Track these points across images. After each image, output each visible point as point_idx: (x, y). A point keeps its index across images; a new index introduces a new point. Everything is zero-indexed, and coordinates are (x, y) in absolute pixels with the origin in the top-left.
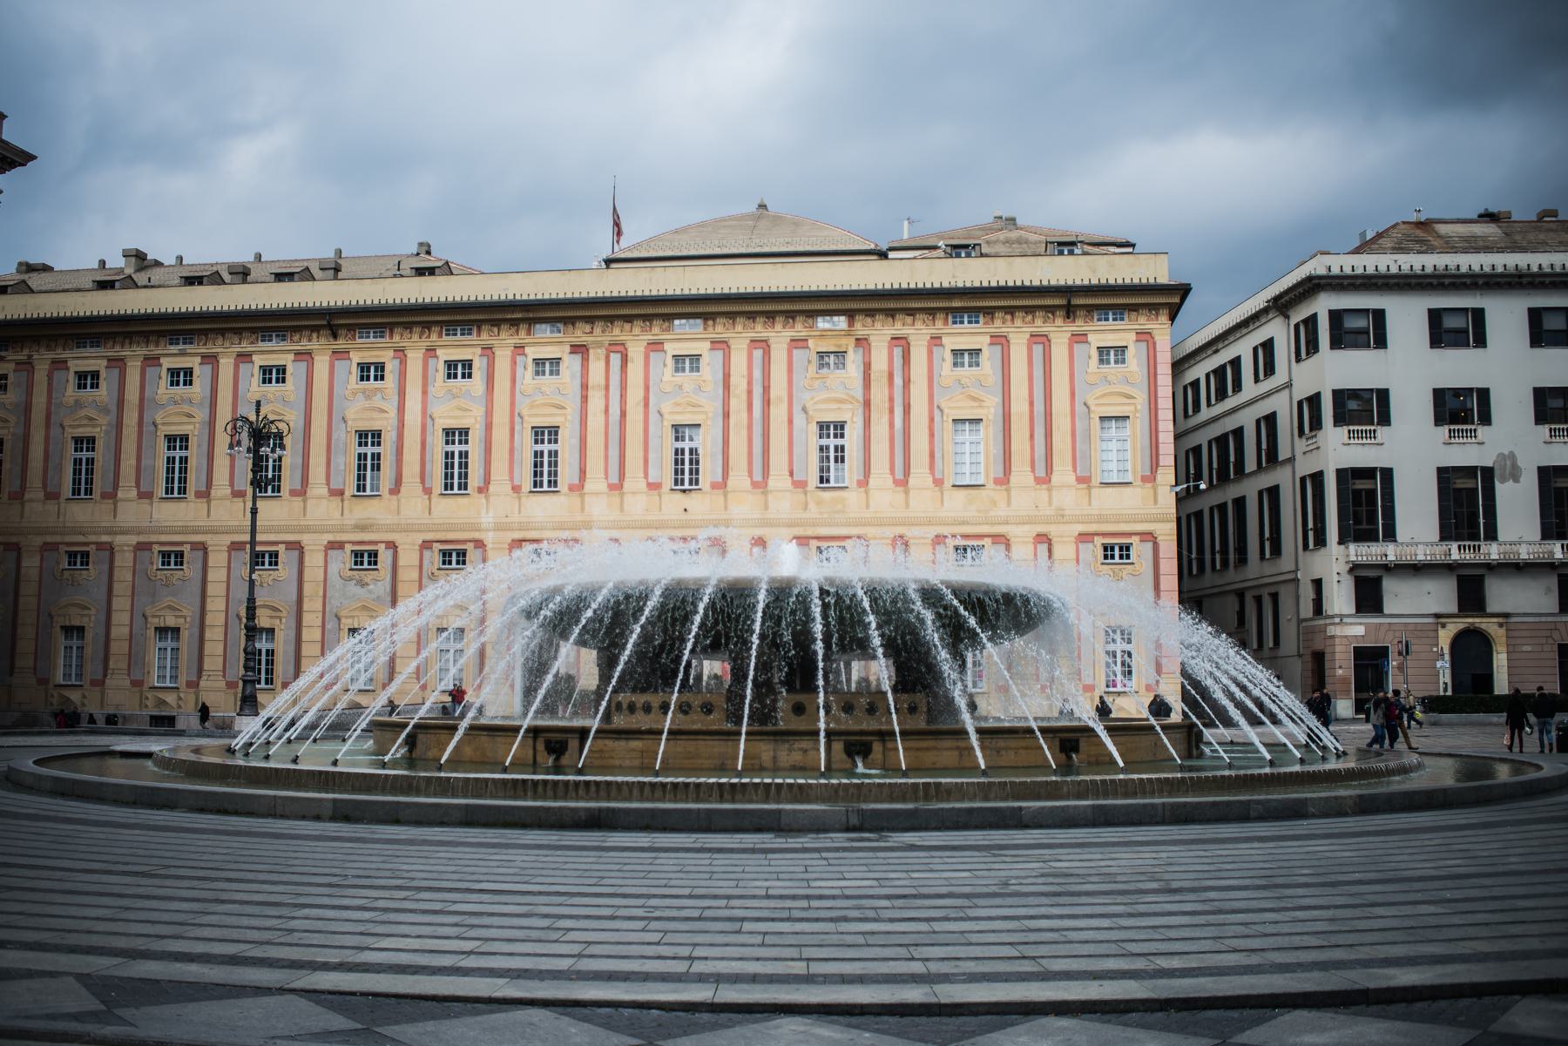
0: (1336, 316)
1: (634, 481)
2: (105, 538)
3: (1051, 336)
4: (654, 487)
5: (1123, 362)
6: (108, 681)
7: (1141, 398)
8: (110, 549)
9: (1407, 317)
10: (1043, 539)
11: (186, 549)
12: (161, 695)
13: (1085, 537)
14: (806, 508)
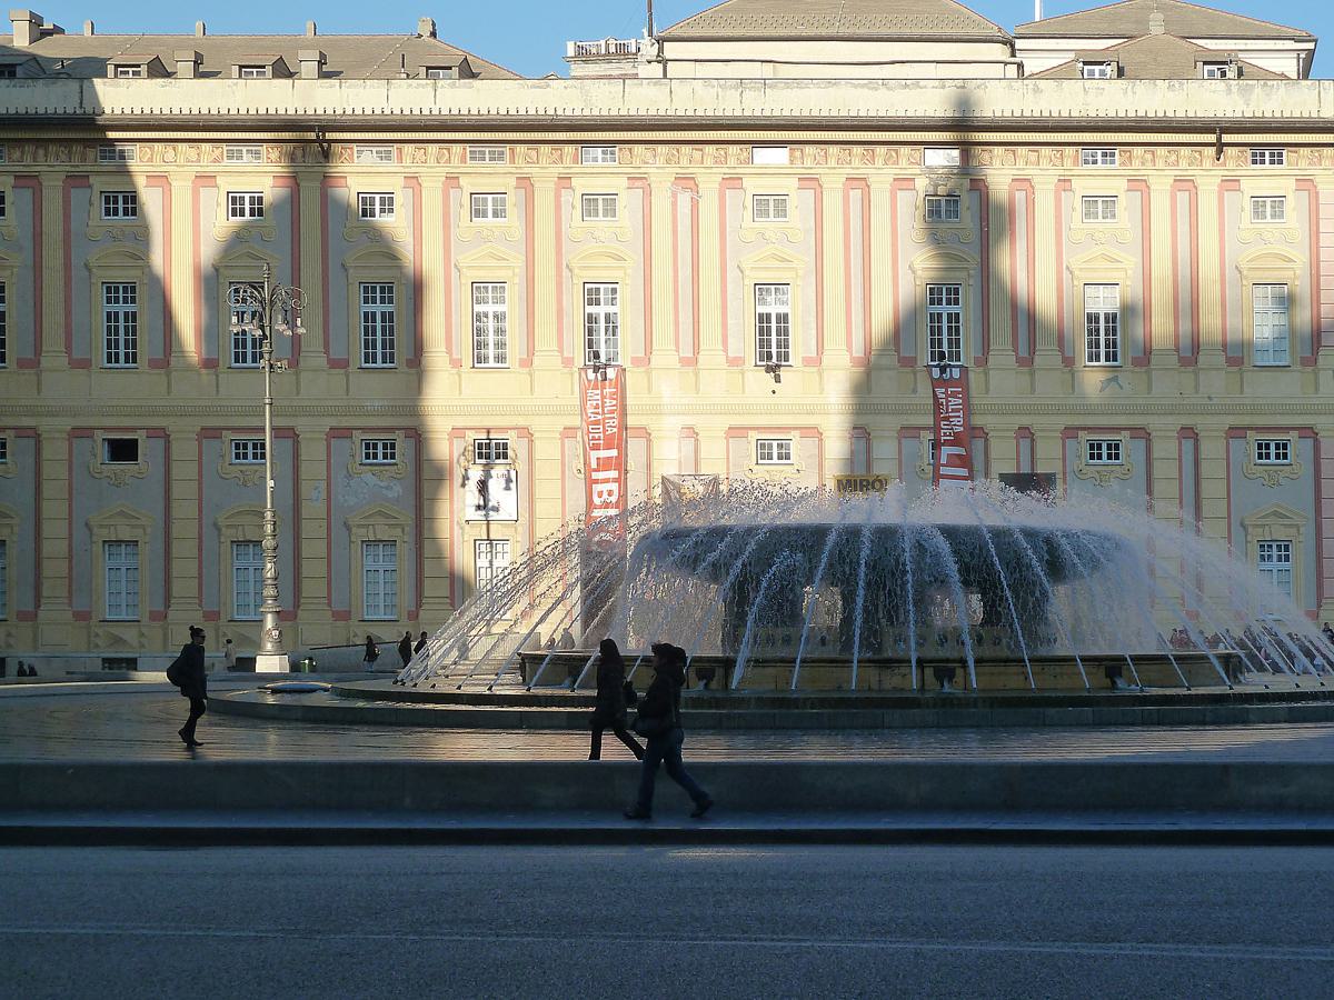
1: (711, 355)
2: (26, 422)
4: (735, 362)
6: (41, 614)
8: (34, 435)
10: (1189, 433)
11: (140, 436)
12: (117, 631)
13: (1236, 432)
14: (915, 391)
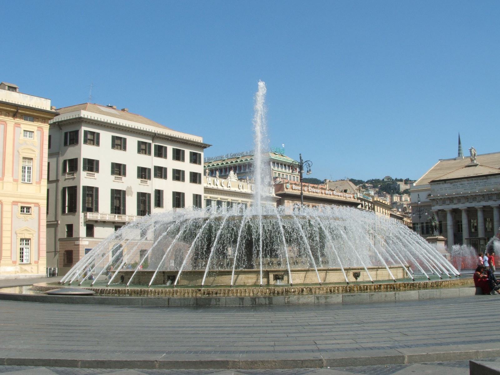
0: (86, 132)
3: (8, 122)
5: (32, 137)
7: (38, 151)
9: (106, 137)
13: (15, 203)
